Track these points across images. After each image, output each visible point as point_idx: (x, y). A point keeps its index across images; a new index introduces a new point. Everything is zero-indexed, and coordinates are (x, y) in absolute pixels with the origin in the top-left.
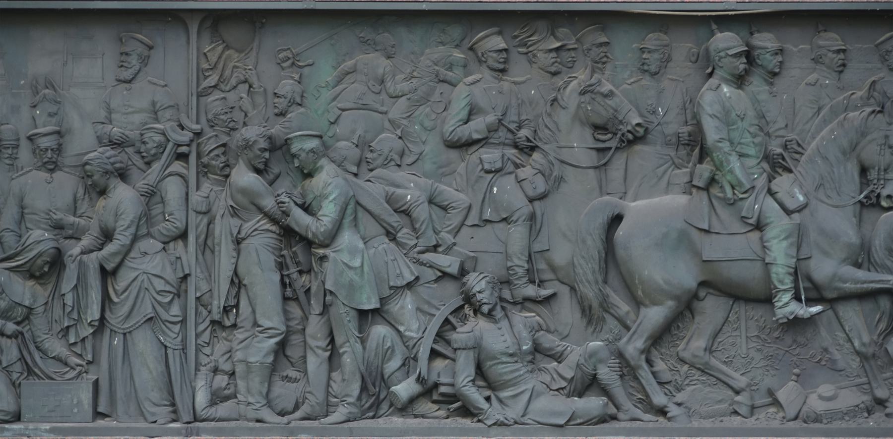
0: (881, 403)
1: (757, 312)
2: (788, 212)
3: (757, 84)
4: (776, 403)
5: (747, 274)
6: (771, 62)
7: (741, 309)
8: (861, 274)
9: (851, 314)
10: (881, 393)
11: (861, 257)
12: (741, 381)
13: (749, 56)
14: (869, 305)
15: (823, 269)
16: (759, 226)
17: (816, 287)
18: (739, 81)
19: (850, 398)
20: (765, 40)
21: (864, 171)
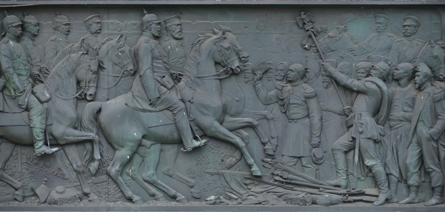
0: (86, 195)
1: (26, 151)
2: (42, 102)
3: (26, 40)
4: (35, 195)
5: (21, 132)
6: (34, 30)
7: (19, 149)
8: (77, 132)
9: (73, 152)
10: (86, 190)
11: (77, 124)
12: (18, 184)
13: (23, 26)
14: (80, 147)
15: (60, 130)
16: (27, 109)
17: (55, 138)
18: (18, 39)
19: (71, 192)
20: (31, 19)
21: (78, 82)
